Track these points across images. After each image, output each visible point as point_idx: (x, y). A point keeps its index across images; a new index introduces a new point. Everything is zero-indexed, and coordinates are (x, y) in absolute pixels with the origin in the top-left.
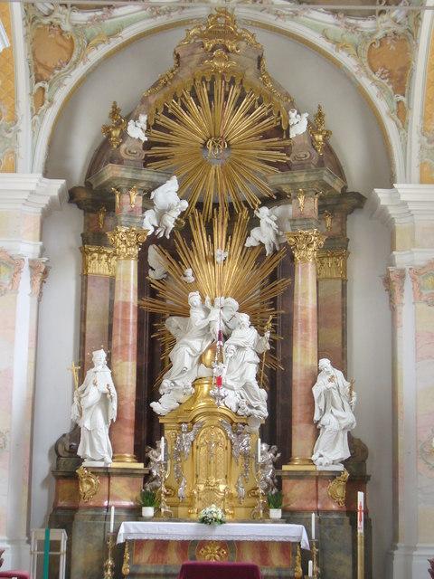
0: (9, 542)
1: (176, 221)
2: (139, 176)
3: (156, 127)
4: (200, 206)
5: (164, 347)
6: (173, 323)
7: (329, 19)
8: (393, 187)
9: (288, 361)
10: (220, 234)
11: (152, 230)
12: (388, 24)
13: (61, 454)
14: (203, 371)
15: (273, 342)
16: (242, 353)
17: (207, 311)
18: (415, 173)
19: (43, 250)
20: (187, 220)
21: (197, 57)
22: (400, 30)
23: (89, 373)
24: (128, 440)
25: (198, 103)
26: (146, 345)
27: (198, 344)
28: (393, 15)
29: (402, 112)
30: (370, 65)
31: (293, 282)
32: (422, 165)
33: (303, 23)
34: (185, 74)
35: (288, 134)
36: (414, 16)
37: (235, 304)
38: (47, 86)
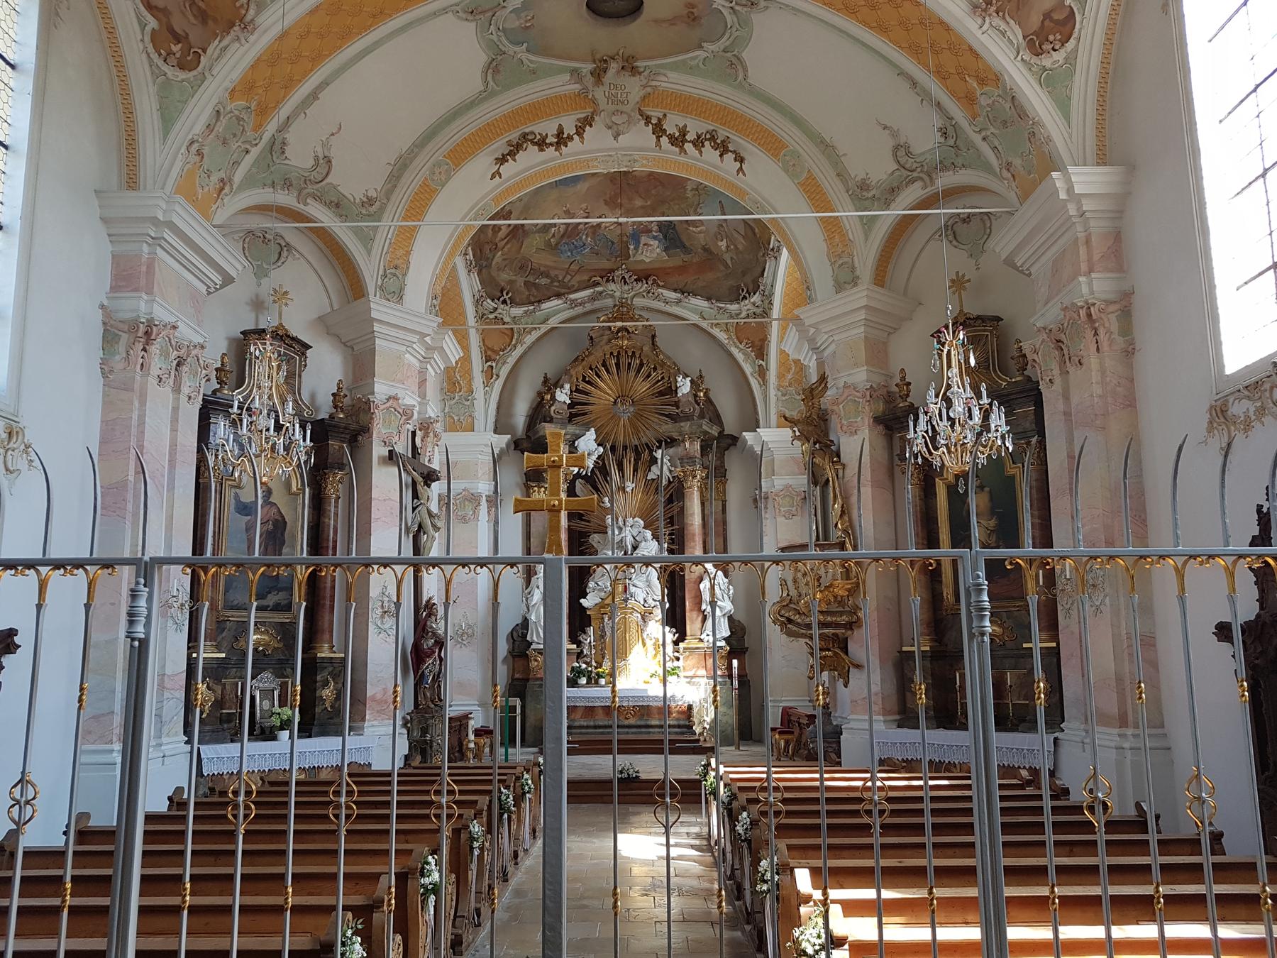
0: (479, 706)
3: (577, 391)
4: (613, 448)
7: (705, 304)
10: (629, 470)
12: (749, 307)
18: (774, 418)
20: (603, 460)
21: (606, 338)
23: (533, 579)
25: (608, 372)
28: (752, 300)
30: (738, 338)
33: (685, 308)
36: (767, 302)
38: (494, 364)
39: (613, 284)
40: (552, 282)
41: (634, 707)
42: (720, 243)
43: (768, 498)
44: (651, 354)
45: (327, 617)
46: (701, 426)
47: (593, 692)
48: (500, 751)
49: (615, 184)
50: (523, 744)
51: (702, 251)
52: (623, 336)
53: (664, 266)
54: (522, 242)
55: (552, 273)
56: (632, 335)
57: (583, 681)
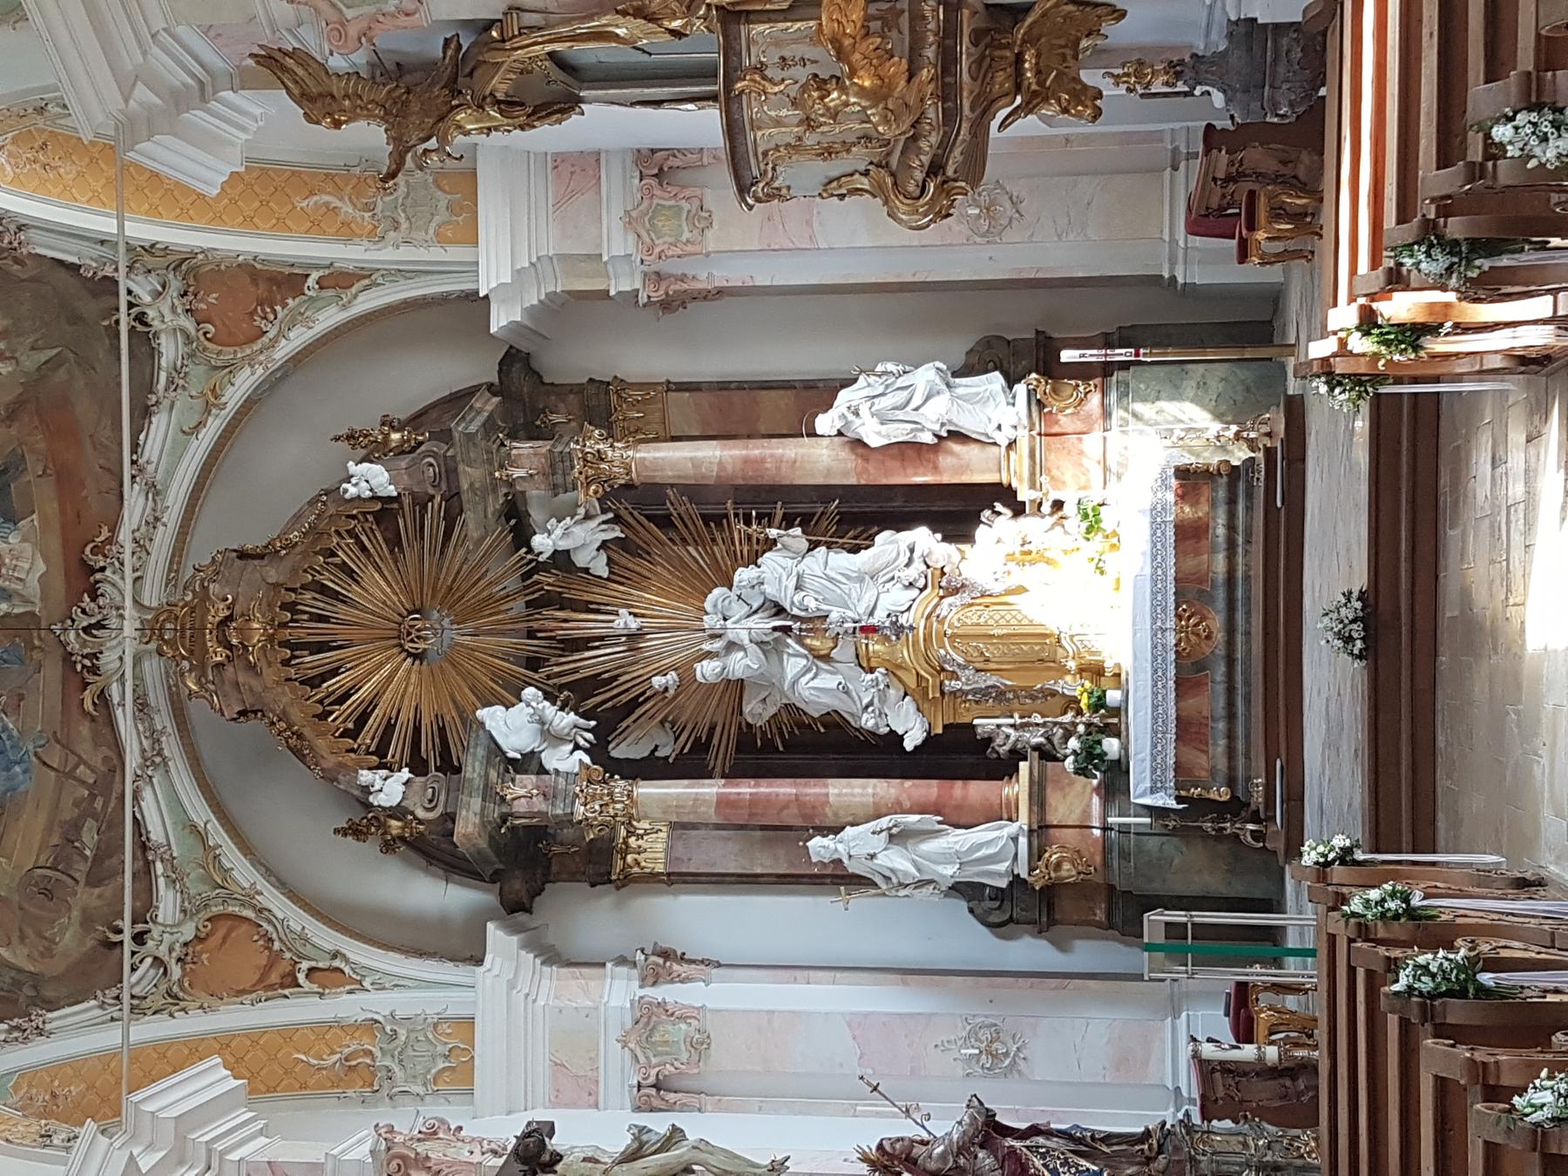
0: (1176, 1016)
1: (562, 709)
2: (476, 782)
3: (381, 751)
4: (533, 663)
5: (800, 725)
6: (756, 711)
8: (486, 297)
9: (825, 492)
10: (589, 625)
11: (580, 755)
12: (166, 311)
13: (1007, 917)
14: (844, 652)
15: (788, 522)
16: (807, 581)
17: (732, 646)
18: (455, 253)
19: (622, 961)
20: (561, 687)
22: (175, 285)
23: (853, 867)
24: (977, 791)
25: (335, 672)
26: (797, 759)
27: (793, 665)
28: (147, 299)
29: (340, 280)
31: (672, 486)
32: (442, 240)
33: (170, 474)
34: (284, 697)
35: (390, 499)
36: (147, 258)
38: (305, 965)
40: (95, 816)
41: (1179, 617)
43: (657, 273)
44: (287, 565)
46: (470, 437)
47: (1139, 722)
48: (1293, 970)
50: (1273, 904)
51: (16, 425)
52: (238, 630)
55: (68, 813)
57: (1111, 746)
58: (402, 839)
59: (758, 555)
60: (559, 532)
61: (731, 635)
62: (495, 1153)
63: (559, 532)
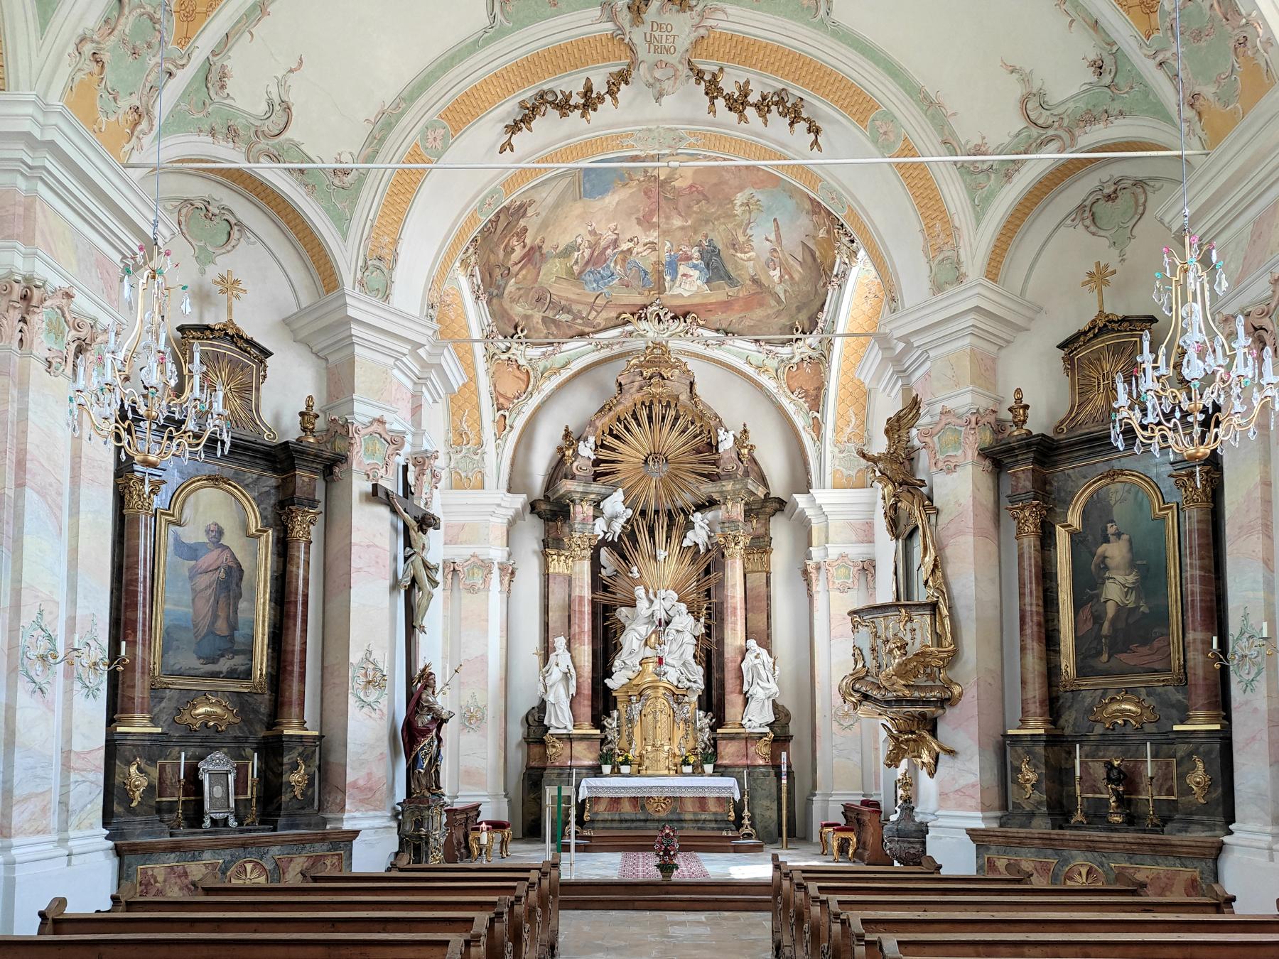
3: (603, 446)
6: (623, 612)
9: (721, 642)
14: (648, 652)
15: (708, 627)
16: (680, 635)
19: (510, 555)
21: (636, 384)
25: (639, 425)
26: (600, 631)
30: (789, 387)
32: (835, 472)
33: (729, 351)
37: (676, 596)
38: (507, 414)
39: (644, 322)
40: (574, 319)
42: (772, 273)
45: (295, 686)
49: (649, 198)
53: (705, 301)
54: (540, 268)
55: (575, 308)
56: (667, 382)
58: (564, 455)
59: (693, 613)
60: (703, 525)
61: (656, 602)
62: (426, 504)
63: (703, 525)
